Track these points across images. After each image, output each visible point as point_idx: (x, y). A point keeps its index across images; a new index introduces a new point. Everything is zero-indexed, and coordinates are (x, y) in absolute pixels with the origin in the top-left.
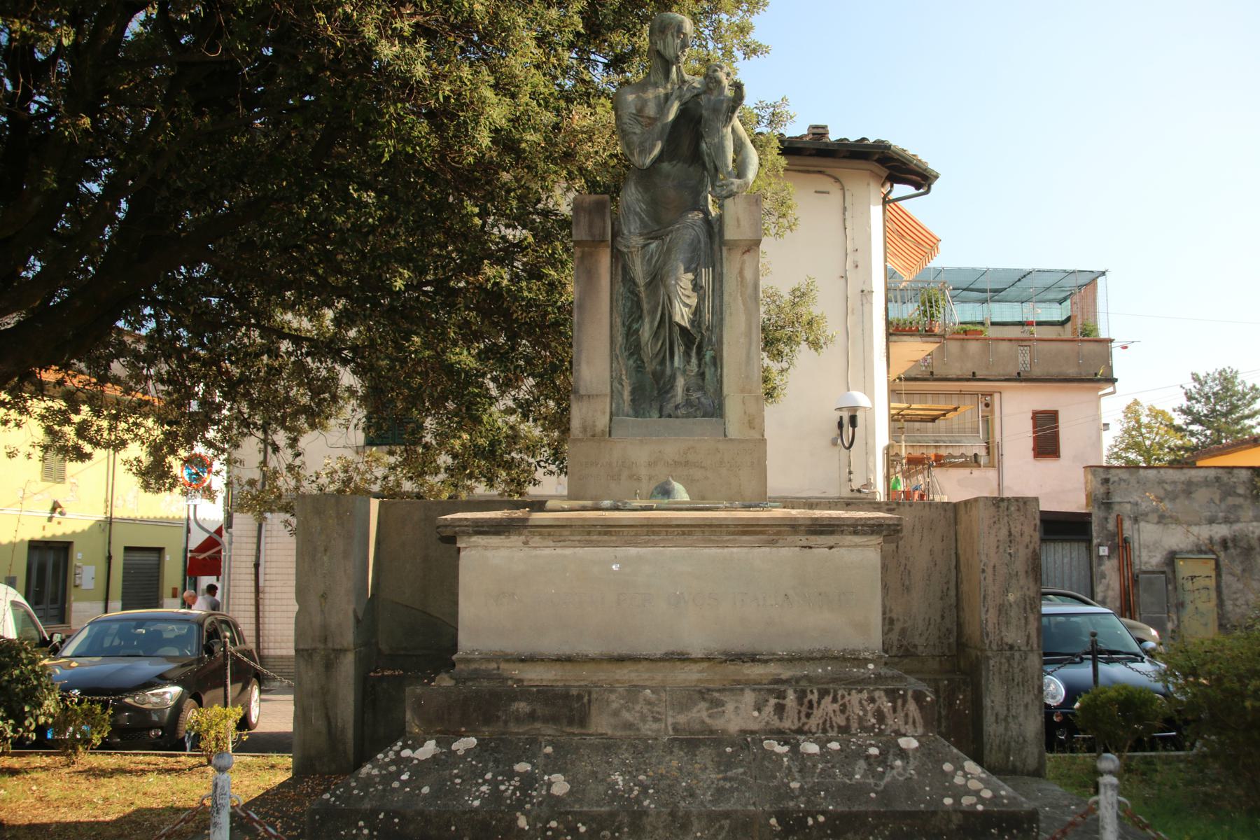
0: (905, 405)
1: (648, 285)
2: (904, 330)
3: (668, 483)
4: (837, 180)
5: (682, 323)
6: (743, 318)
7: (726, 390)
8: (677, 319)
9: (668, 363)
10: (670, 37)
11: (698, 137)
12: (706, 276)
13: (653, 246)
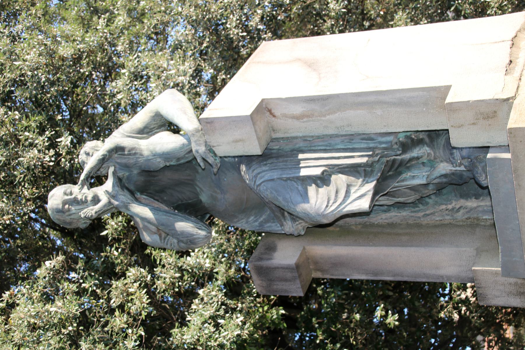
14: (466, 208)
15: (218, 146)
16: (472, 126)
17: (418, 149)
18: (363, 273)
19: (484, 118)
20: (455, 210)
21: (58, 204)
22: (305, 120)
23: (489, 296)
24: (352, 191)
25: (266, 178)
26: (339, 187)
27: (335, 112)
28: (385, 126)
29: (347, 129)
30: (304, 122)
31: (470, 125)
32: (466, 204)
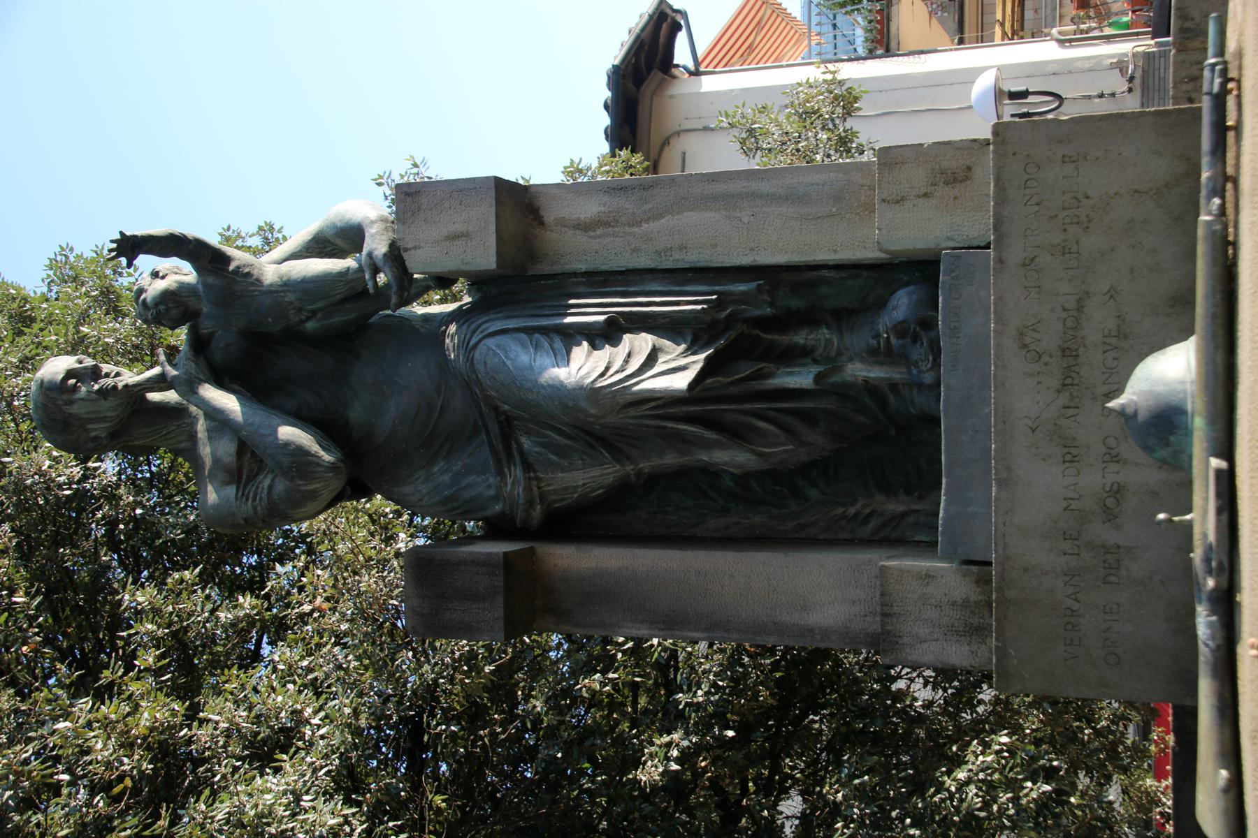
0: (998, 30)
1: (616, 453)
2: (881, 32)
3: (1126, 417)
4: (666, 142)
5: (698, 367)
6: (692, 218)
7: (871, 254)
8: (680, 382)
9: (809, 405)
10: (74, 409)
11: (293, 337)
12: (588, 312)
13: (526, 442)
15: (415, 248)
19: (947, 183)
21: (57, 373)
22: (598, 232)
23: (906, 640)
24: (660, 360)
25: (491, 330)
26: (637, 349)
27: (661, 216)
28: (752, 249)
29: (677, 257)
30: (595, 238)
31: (919, 197)
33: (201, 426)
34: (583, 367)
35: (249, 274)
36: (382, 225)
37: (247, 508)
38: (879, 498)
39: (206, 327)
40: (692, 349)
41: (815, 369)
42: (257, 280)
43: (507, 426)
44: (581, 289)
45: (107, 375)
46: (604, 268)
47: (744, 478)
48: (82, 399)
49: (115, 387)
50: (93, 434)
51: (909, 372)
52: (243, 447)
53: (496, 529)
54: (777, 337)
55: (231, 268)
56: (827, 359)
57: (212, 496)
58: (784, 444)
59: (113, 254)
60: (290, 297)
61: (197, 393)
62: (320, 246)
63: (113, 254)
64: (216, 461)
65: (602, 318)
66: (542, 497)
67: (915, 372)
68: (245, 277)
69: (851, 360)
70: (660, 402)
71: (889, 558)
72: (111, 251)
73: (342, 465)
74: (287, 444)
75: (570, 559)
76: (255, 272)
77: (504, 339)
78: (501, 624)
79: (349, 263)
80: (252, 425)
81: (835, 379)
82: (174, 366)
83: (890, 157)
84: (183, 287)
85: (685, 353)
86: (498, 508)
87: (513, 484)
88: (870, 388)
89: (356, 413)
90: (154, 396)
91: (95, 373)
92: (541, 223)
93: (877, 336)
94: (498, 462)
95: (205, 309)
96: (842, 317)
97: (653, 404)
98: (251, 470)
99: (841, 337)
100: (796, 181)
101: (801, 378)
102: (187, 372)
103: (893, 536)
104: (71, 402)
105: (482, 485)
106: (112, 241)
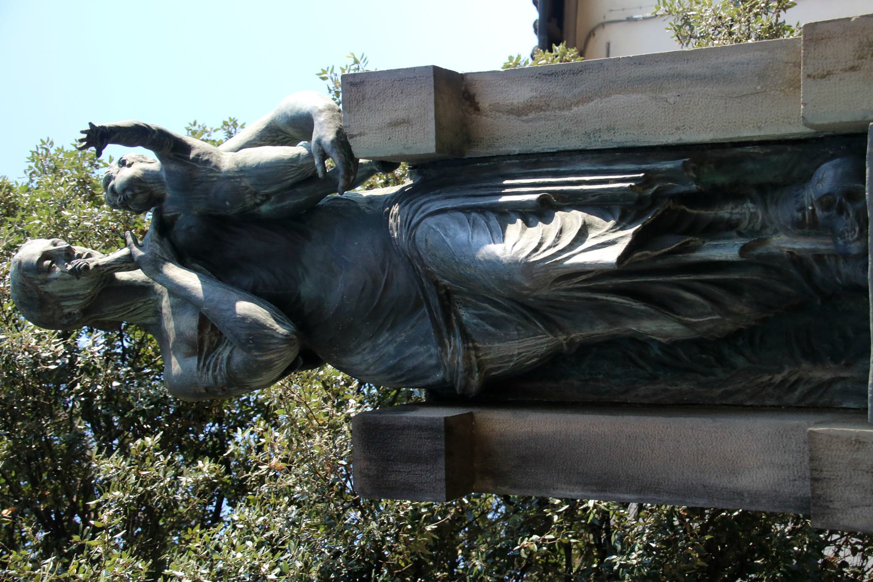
1: (551, 325)
4: (592, 33)
5: (626, 242)
6: (619, 100)
7: (796, 129)
8: (610, 256)
9: (735, 276)
10: (50, 288)
11: (249, 219)
12: (522, 192)
13: (465, 315)
14: (808, 382)
15: (360, 134)
16: (848, 74)
17: (731, 205)
18: (577, 483)
20: (787, 385)
21: (34, 255)
22: (531, 116)
23: (837, 505)
24: (590, 236)
25: (432, 209)
26: (568, 225)
27: (590, 99)
28: (678, 129)
29: (605, 137)
30: (527, 121)
31: (845, 71)
32: (811, 374)
33: (166, 303)
34: (517, 243)
35: (208, 162)
36: (330, 114)
37: (208, 378)
38: (805, 365)
39: (169, 210)
40: (621, 225)
41: (740, 242)
42: (216, 167)
43: (447, 300)
44: (514, 170)
45: (80, 256)
46: (536, 150)
47: (672, 347)
48: (56, 279)
49: (87, 267)
50: (67, 311)
51: (835, 243)
52: (204, 321)
53: (439, 395)
54: (703, 212)
55: (192, 156)
56: (752, 232)
57: (176, 367)
58: (710, 314)
59: (84, 143)
60: (246, 182)
61: (161, 272)
62: (273, 134)
63: (84, 143)
64: (179, 334)
65: (535, 197)
66: (480, 365)
67: (840, 242)
68: (204, 163)
69: (776, 232)
70: (591, 275)
71: (817, 424)
72: (82, 141)
73: (295, 337)
74: (244, 318)
75: (505, 424)
76: (214, 159)
77: (443, 218)
78: (443, 485)
79: (300, 149)
80: (212, 300)
81: (760, 250)
82: (140, 247)
83: (815, 33)
84: (147, 173)
85: (614, 229)
86: (439, 376)
87: (453, 353)
88: (796, 259)
89: (307, 289)
90: (122, 276)
91: (69, 255)
92: (477, 109)
93: (802, 209)
94: (438, 332)
95: (168, 195)
96: (766, 192)
97: (584, 277)
98: (211, 343)
99: (766, 209)
100: (720, 60)
101: (726, 251)
102: (152, 253)
103: (819, 403)
104: (47, 282)
105: (424, 354)
106: (82, 132)
